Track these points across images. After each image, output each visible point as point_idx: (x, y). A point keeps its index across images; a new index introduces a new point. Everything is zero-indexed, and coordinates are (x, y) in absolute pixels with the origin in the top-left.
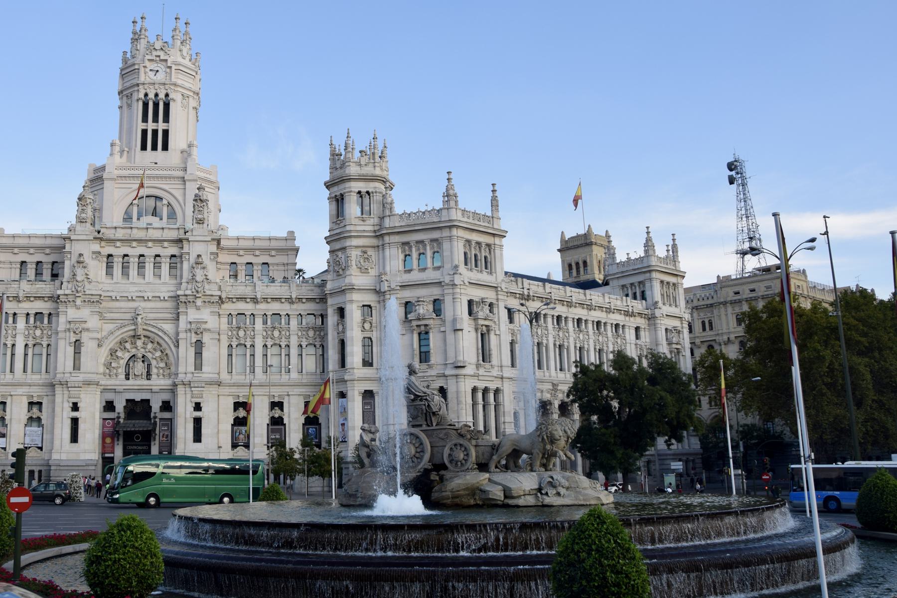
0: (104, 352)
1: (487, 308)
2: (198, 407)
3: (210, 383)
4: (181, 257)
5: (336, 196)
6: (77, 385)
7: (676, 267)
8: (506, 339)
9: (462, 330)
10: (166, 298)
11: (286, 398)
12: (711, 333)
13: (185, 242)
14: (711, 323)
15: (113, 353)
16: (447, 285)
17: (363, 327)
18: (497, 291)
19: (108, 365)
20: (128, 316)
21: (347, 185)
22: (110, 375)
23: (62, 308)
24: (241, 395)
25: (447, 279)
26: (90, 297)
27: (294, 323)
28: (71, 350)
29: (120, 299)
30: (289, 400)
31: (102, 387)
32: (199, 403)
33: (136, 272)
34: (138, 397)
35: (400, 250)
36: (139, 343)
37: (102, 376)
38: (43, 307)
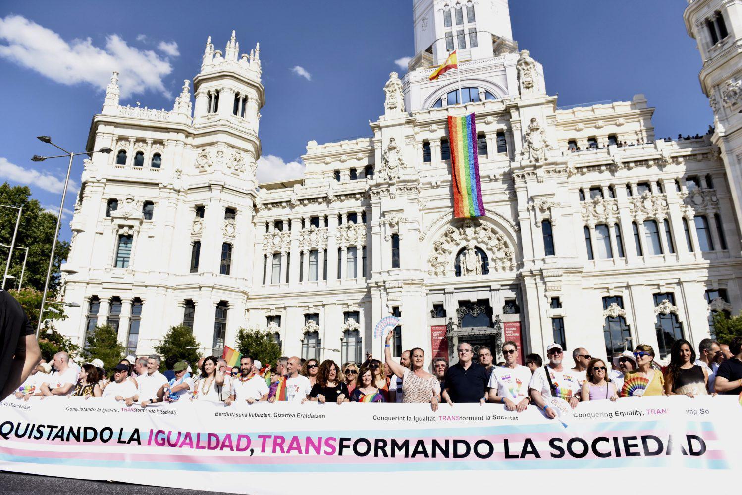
2: (556, 302)
3: (570, 271)
4: (510, 129)
6: (396, 285)
13: (513, 111)
19: (434, 263)
22: (436, 274)
26: (406, 183)
27: (670, 187)
29: (441, 184)
34: (473, 297)
38: (356, 206)
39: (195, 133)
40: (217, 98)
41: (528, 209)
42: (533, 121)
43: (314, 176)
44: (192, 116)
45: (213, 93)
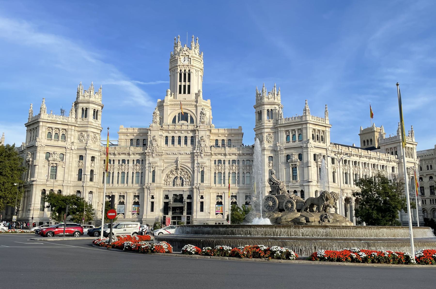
0: (164, 176)
1: (322, 157)
2: (202, 197)
5: (258, 111)
6: (153, 189)
7: (412, 140)
8: (330, 171)
9: (311, 166)
10: (189, 154)
11: (238, 194)
12: (431, 170)
14: (431, 166)
15: (168, 176)
16: (305, 148)
17: (269, 165)
18: (327, 151)
19: (166, 181)
20: (174, 161)
21: (263, 107)
22: (167, 185)
23: (147, 157)
24: (219, 192)
25: (305, 145)
28: (151, 175)
30: (239, 195)
31: (163, 189)
32: (203, 196)
33: (177, 143)
35: (285, 134)
36: (179, 172)
37: (163, 185)
39: (78, 126)
40: (86, 110)
41: (197, 167)
42: (202, 136)
43: (122, 141)
44: (76, 118)
45: (85, 109)
